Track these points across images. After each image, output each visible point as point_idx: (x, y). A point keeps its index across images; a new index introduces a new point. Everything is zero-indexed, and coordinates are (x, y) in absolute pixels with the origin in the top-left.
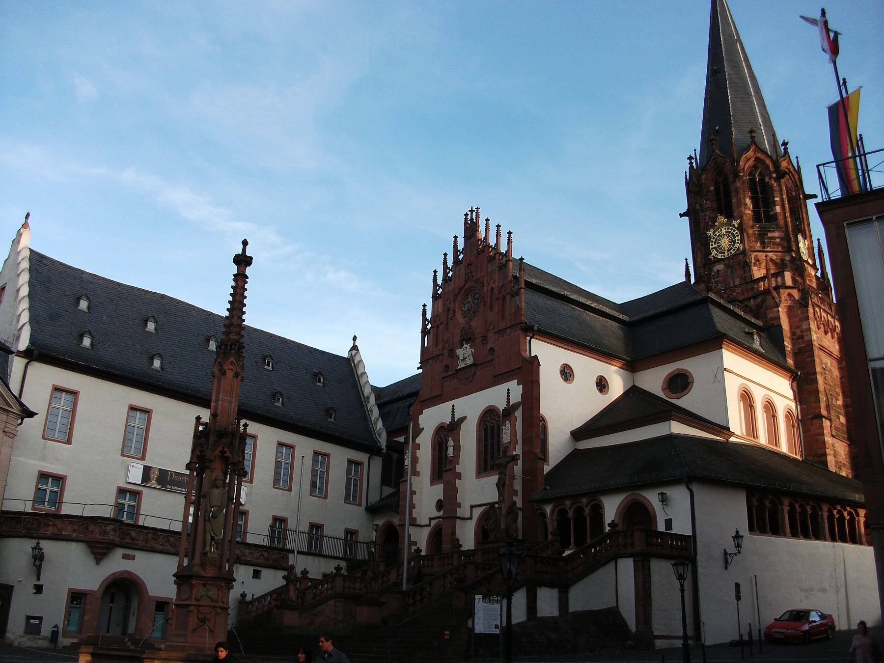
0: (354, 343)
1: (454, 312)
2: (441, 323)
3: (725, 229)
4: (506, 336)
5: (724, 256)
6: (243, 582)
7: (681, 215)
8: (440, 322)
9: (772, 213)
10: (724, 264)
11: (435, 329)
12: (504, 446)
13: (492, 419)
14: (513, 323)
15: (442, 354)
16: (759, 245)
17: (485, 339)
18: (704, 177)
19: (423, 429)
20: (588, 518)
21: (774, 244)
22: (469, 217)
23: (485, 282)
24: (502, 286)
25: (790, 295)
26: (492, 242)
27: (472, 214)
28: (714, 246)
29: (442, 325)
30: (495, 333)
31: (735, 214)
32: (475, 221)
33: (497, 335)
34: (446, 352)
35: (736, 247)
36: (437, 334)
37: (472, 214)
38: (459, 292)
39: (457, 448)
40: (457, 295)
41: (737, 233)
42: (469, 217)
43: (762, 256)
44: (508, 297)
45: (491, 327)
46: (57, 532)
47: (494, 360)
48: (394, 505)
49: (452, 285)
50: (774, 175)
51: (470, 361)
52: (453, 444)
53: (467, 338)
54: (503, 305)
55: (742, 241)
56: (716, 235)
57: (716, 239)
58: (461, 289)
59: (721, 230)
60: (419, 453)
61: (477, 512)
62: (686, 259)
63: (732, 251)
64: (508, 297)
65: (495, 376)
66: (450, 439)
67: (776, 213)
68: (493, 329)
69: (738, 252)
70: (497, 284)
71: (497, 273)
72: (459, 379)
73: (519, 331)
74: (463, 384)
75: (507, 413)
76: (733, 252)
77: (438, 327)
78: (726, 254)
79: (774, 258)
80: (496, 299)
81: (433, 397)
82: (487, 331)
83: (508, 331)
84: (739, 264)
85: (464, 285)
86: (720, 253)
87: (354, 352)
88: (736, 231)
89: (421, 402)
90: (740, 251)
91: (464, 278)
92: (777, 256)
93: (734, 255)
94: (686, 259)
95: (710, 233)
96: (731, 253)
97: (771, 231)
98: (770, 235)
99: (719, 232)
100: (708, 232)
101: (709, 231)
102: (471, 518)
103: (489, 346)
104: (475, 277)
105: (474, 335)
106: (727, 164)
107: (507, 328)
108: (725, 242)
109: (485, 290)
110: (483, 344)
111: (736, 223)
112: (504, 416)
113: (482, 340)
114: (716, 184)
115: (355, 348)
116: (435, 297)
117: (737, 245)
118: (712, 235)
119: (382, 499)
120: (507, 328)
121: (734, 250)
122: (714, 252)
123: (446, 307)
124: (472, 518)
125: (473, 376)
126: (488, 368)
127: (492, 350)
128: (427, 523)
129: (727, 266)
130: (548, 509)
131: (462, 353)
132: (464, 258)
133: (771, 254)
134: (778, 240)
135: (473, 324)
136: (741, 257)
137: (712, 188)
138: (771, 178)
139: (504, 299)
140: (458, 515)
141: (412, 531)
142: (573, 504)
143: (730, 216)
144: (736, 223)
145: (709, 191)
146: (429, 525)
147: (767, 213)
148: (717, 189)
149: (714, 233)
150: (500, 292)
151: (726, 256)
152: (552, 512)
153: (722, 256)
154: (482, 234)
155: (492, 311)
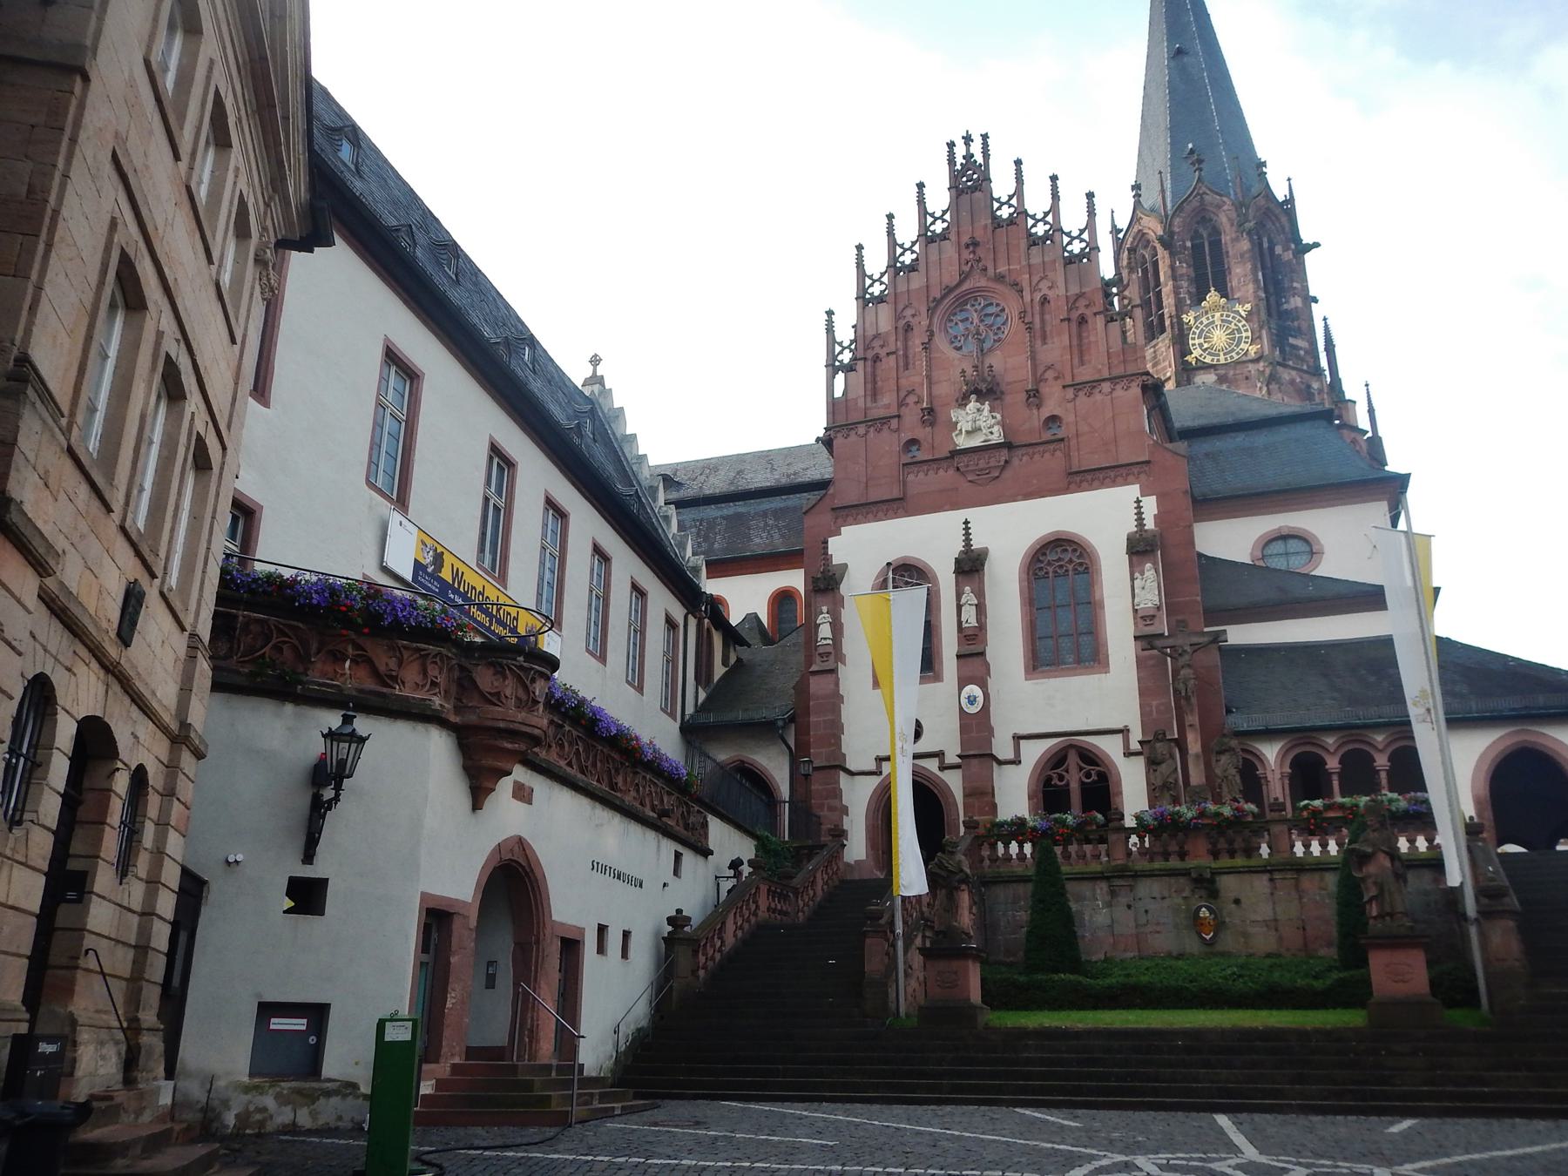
0: (595, 371)
3: (1222, 315)
4: (1098, 397)
5: (1218, 360)
6: (665, 885)
8: (886, 350)
9: (1285, 306)
10: (1216, 375)
11: (869, 363)
12: (1140, 614)
15: (899, 416)
16: (1278, 353)
17: (1035, 395)
18: (1177, 221)
19: (845, 566)
20: (1383, 775)
21: (1298, 357)
22: (960, 151)
23: (1025, 285)
26: (1037, 202)
28: (1197, 342)
29: (893, 357)
30: (1064, 387)
32: (979, 158)
33: (1070, 393)
34: (911, 415)
35: (1242, 350)
36: (874, 375)
38: (943, 297)
39: (981, 609)
40: (938, 302)
41: (1243, 326)
42: (960, 151)
44: (1100, 321)
45: (1050, 375)
46: (370, 685)
48: (780, 723)
49: (917, 281)
50: (1293, 246)
51: (997, 437)
52: (976, 602)
53: (986, 390)
54: (1080, 337)
56: (1201, 323)
57: (1202, 330)
58: (949, 290)
59: (1213, 317)
60: (847, 615)
61: (1033, 753)
63: (1233, 354)
65: (1070, 474)
66: (967, 589)
67: (1296, 308)
68: (1056, 378)
69: (1244, 358)
70: (1061, 291)
72: (958, 469)
73: (1136, 390)
74: (970, 481)
75: (1148, 548)
76: (1236, 357)
77: (877, 359)
78: (1222, 358)
79: (1298, 380)
81: (870, 504)
83: (1106, 386)
86: (1209, 354)
87: (596, 388)
88: (1244, 322)
89: (833, 509)
90: (1249, 358)
92: (1301, 378)
93: (1237, 363)
95: (1188, 318)
96: (1232, 357)
97: (1292, 336)
98: (1291, 340)
99: (1208, 319)
100: (1184, 316)
102: (1016, 761)
103: (1046, 412)
104: (991, 272)
105: (998, 384)
106: (1225, 208)
107: (1104, 380)
108: (1219, 337)
109: (1027, 297)
111: (1243, 309)
112: (1137, 553)
113: (1029, 397)
114: (1196, 236)
115: (596, 380)
116: (863, 299)
117: (1243, 345)
118: (1192, 322)
119: (697, 711)
120: (1104, 380)
121: (1238, 353)
122: (1196, 353)
123: (902, 323)
124: (1020, 762)
125: (1003, 468)
126: (1047, 455)
127: (1053, 419)
128: (872, 766)
129: (1222, 379)
130: (1270, 752)
131: (970, 418)
133: (1294, 373)
134: (1302, 353)
135: (996, 360)
137: (1189, 244)
138: (1286, 249)
139: (1082, 320)
140: (994, 753)
141: (844, 779)
142: (1344, 743)
143: (1224, 295)
145: (1185, 248)
146: (878, 773)
147: (1279, 304)
148: (1197, 249)
151: (1222, 361)
152: (1283, 755)
153: (1213, 360)
154: (1002, 185)
155: (1045, 343)
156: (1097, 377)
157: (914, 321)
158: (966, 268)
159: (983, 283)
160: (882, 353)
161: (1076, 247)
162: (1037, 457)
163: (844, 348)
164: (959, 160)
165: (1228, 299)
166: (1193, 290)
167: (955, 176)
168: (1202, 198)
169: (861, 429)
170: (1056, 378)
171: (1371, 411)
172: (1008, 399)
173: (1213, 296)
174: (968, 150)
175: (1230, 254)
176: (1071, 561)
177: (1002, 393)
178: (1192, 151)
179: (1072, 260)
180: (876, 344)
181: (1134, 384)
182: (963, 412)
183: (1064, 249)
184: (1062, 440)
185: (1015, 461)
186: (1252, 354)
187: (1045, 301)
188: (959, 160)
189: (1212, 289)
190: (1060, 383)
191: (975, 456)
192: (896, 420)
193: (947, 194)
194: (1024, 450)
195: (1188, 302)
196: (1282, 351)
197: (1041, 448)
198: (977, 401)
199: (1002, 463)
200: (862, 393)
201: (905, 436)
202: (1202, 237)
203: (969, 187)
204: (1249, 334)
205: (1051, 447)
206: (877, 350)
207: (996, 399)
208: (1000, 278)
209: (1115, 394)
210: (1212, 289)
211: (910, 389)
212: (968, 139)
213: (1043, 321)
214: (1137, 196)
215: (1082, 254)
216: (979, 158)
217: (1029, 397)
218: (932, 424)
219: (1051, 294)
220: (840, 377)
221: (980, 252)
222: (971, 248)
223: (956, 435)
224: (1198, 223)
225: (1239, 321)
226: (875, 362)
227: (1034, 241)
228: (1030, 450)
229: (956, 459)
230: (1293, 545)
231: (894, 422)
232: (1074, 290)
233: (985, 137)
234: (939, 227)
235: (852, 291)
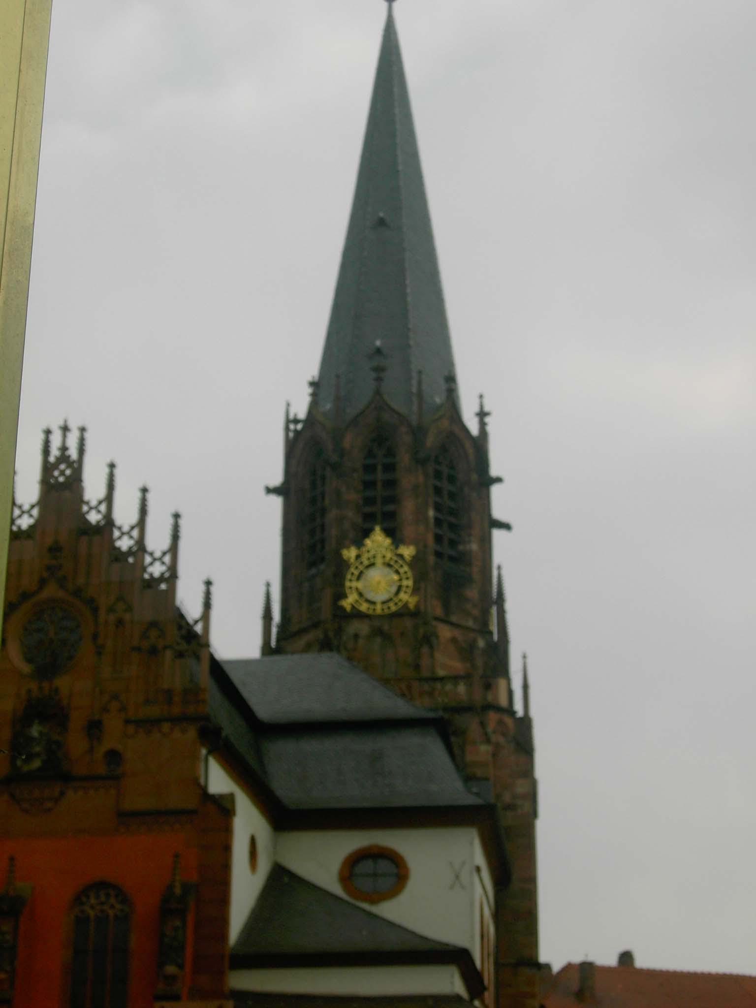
7: (269, 491)
13: (102, 903)
25: (501, 722)
27: (64, 437)
30: (127, 722)
37: (64, 437)
43: (445, 632)
44: (169, 654)
55: (416, 590)
62: (268, 585)
64: (169, 654)
73: (192, 733)
82: (105, 710)
83: (166, 727)
84: (402, 634)
88: (406, 568)
94: (268, 585)
95: (350, 553)
101: (348, 547)
103: (107, 744)
111: (408, 551)
129: (378, 632)
136: (408, 623)
139: (154, 651)
143: (389, 532)
144: (408, 551)
149: (358, 557)
158: (45, 575)
159: (61, 594)
161: (157, 570)
164: (55, 452)
167: (47, 468)
171: (526, 687)
174: (64, 441)
176: (112, 907)
178: (378, 351)
179: (153, 583)
183: (144, 569)
186: (411, 606)
187: (120, 622)
188: (55, 452)
196: (446, 606)
203: (62, 484)
204: (410, 583)
212: (65, 429)
214: (314, 395)
215: (162, 579)
216: (73, 453)
219: (127, 617)
227: (119, 556)
230: (384, 866)
233: (83, 430)
234: (25, 522)
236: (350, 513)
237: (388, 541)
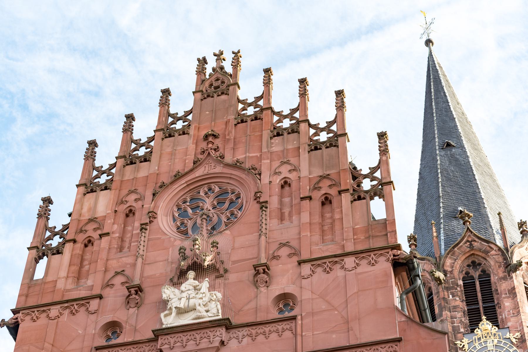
1: (152, 215)
2: (101, 236)
4: (338, 272)
8: (99, 232)
11: (79, 246)
14: (360, 248)
15: (100, 297)
17: (264, 272)
24: (322, 177)
29: (105, 239)
30: (300, 263)
31: (509, 324)
33: (306, 269)
38: (172, 183)
44: (346, 198)
47: (299, 317)
49: (144, 170)
58: (178, 177)
59: (486, 342)
68: (290, 256)
71: (304, 155)
77: (89, 242)
80: (302, 199)
85: (191, 170)
88: (515, 348)
91: (191, 158)
103: (276, 289)
106: (493, 252)
109: (265, 178)
110: (256, 284)
113: (258, 273)
126: (274, 336)
132: (192, 127)
137: (461, 282)
139: (327, 201)
145: (457, 285)
150: (316, 188)
156: (339, 252)
157: (137, 205)
158: (200, 157)
159: (219, 169)
160: (95, 235)
162: (261, 338)
163: (56, 234)
165: (499, 328)
166: (466, 320)
168: (471, 245)
169: (54, 311)
170: (290, 256)
172: (232, 277)
173: (486, 325)
175: (499, 291)
177: (226, 271)
180: (90, 227)
181: (382, 259)
182: (176, 291)
184: (294, 318)
185: (233, 344)
188: (209, 70)
189: (484, 317)
190: (295, 259)
191: (184, 337)
192: (97, 301)
193: (192, 98)
194: (245, 331)
195: (462, 330)
197: (267, 329)
198: (194, 279)
199: (217, 344)
200: (63, 273)
201: (109, 318)
202: (472, 278)
205: (280, 327)
206: (90, 233)
207: (217, 277)
208: (237, 165)
209: (359, 270)
210: (484, 317)
211: (119, 270)
212: (219, 56)
213: (281, 203)
216: (229, 69)
217: (258, 273)
218: (138, 305)
219: (293, 176)
220: (44, 262)
221: (218, 142)
222: (210, 139)
223: (166, 316)
224: (469, 266)
225: (511, 347)
226: (86, 246)
228: (253, 331)
229: (160, 341)
231: (94, 304)
232: (317, 172)
233: (237, 55)
235: (77, 177)
236: (459, 315)
237: (495, 330)
